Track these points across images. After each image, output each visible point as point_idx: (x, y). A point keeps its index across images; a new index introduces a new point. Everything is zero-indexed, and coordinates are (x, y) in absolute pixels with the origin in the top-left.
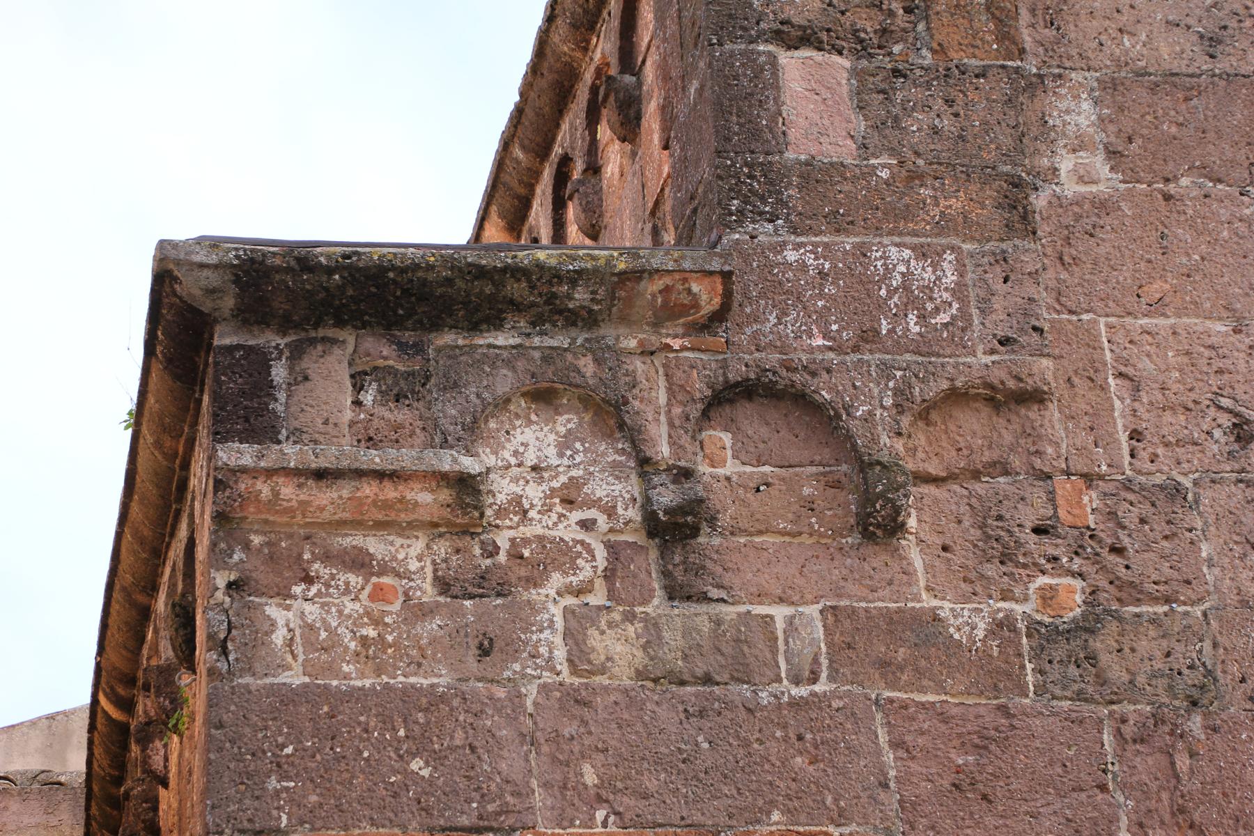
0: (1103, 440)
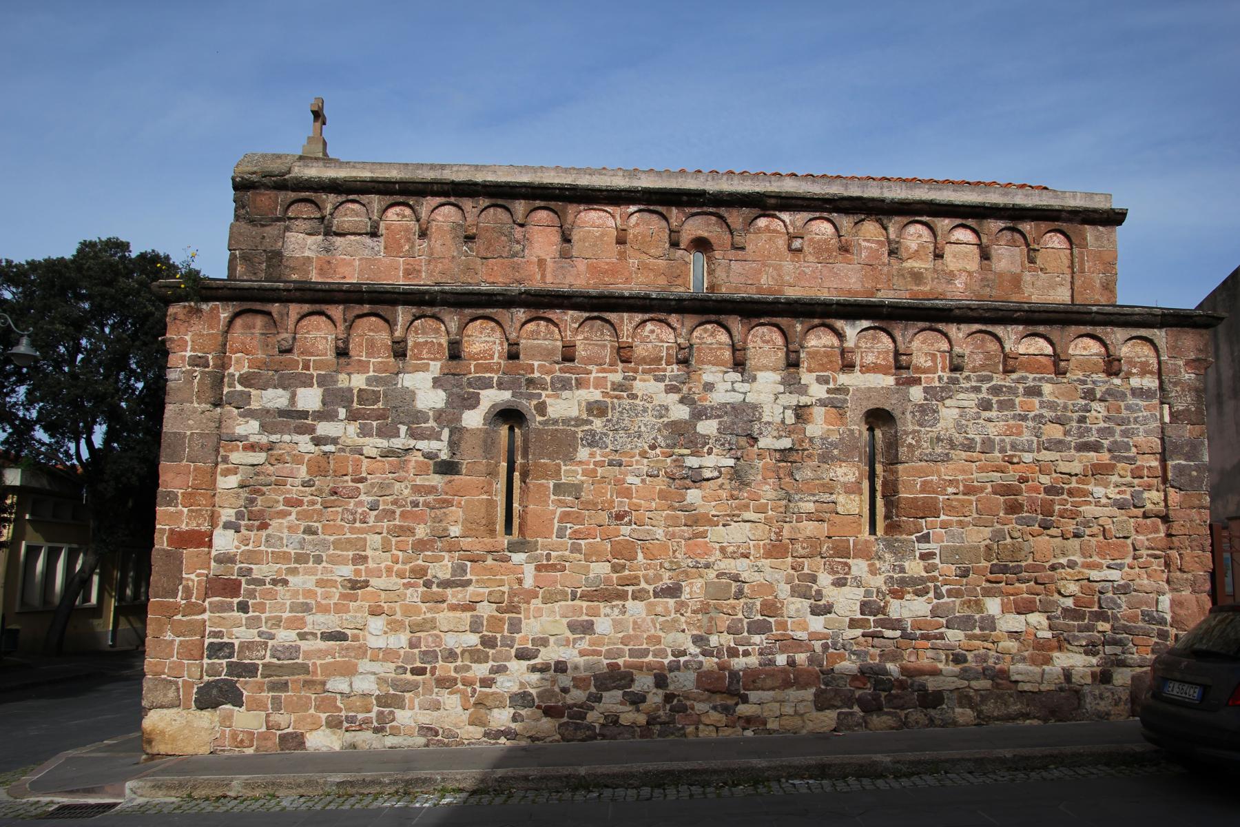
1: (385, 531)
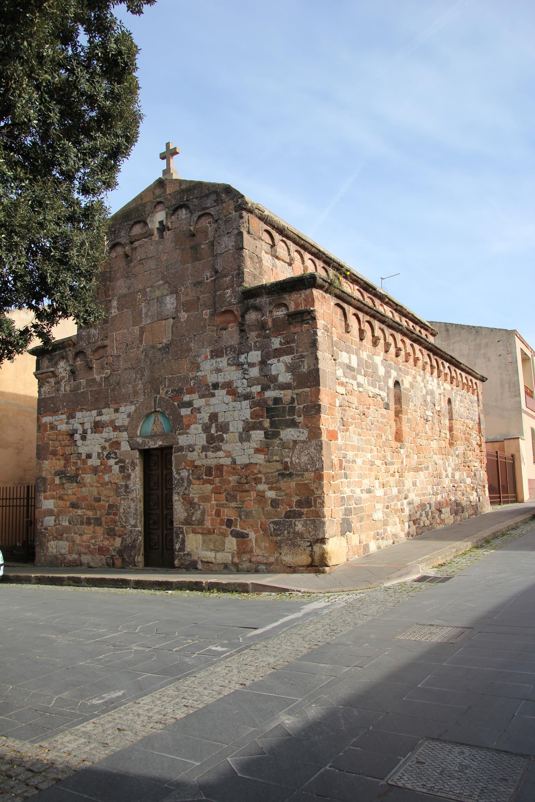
0: (113, 350)
1: (375, 436)
